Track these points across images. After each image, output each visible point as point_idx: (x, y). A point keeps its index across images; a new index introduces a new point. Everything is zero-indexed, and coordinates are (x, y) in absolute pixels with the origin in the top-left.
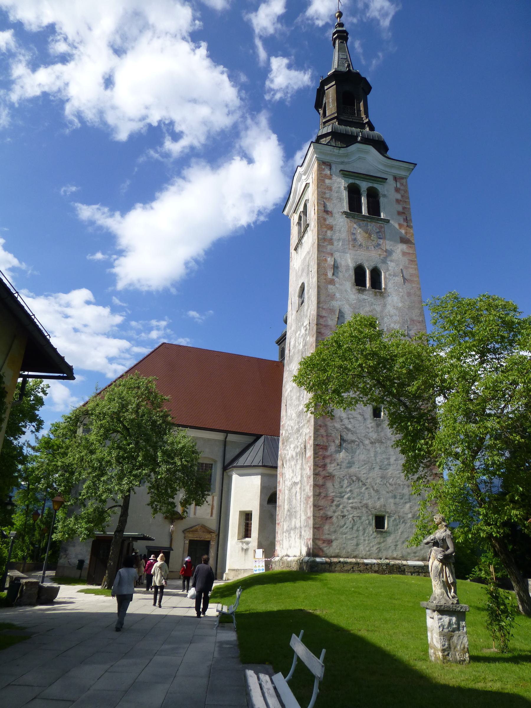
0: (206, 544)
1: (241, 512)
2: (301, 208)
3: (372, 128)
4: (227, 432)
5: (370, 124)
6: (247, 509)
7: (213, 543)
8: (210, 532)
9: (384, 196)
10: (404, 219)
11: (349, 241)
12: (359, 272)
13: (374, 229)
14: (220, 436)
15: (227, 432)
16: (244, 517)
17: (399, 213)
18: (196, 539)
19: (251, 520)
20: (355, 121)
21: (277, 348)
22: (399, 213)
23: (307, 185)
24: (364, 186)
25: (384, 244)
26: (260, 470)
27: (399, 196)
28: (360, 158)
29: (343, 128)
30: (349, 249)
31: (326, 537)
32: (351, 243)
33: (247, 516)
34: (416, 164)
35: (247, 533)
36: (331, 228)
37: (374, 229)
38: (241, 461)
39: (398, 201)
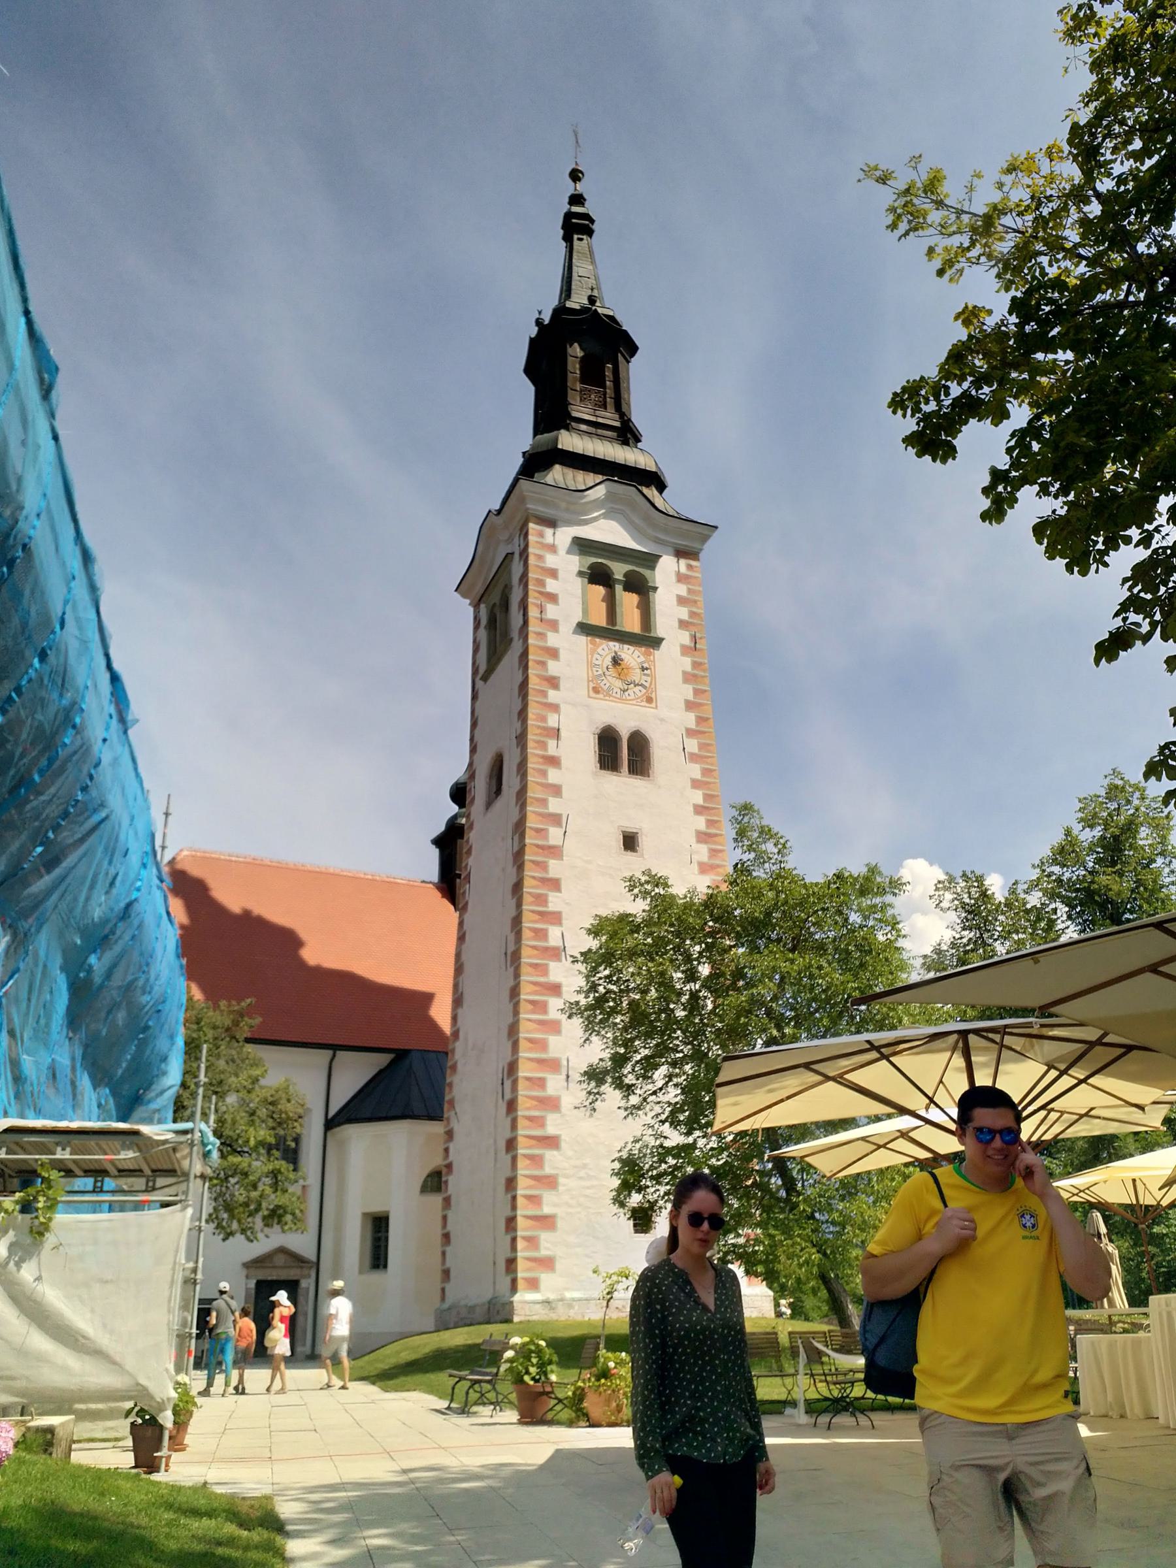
1: (365, 1215)
2: (495, 597)
6: (376, 1208)
8: (298, 1260)
9: (655, 589)
10: (691, 635)
11: (589, 681)
12: (607, 741)
13: (636, 657)
15: (335, 1048)
16: (369, 1227)
17: (683, 624)
18: (269, 1278)
19: (387, 1231)
20: (600, 420)
21: (434, 853)
22: (683, 624)
23: (509, 556)
24: (619, 570)
25: (653, 686)
27: (682, 590)
30: (589, 697)
31: (544, 1252)
32: (592, 685)
33: (379, 1224)
34: (716, 527)
35: (378, 1258)
36: (554, 653)
37: (636, 657)
39: (681, 601)
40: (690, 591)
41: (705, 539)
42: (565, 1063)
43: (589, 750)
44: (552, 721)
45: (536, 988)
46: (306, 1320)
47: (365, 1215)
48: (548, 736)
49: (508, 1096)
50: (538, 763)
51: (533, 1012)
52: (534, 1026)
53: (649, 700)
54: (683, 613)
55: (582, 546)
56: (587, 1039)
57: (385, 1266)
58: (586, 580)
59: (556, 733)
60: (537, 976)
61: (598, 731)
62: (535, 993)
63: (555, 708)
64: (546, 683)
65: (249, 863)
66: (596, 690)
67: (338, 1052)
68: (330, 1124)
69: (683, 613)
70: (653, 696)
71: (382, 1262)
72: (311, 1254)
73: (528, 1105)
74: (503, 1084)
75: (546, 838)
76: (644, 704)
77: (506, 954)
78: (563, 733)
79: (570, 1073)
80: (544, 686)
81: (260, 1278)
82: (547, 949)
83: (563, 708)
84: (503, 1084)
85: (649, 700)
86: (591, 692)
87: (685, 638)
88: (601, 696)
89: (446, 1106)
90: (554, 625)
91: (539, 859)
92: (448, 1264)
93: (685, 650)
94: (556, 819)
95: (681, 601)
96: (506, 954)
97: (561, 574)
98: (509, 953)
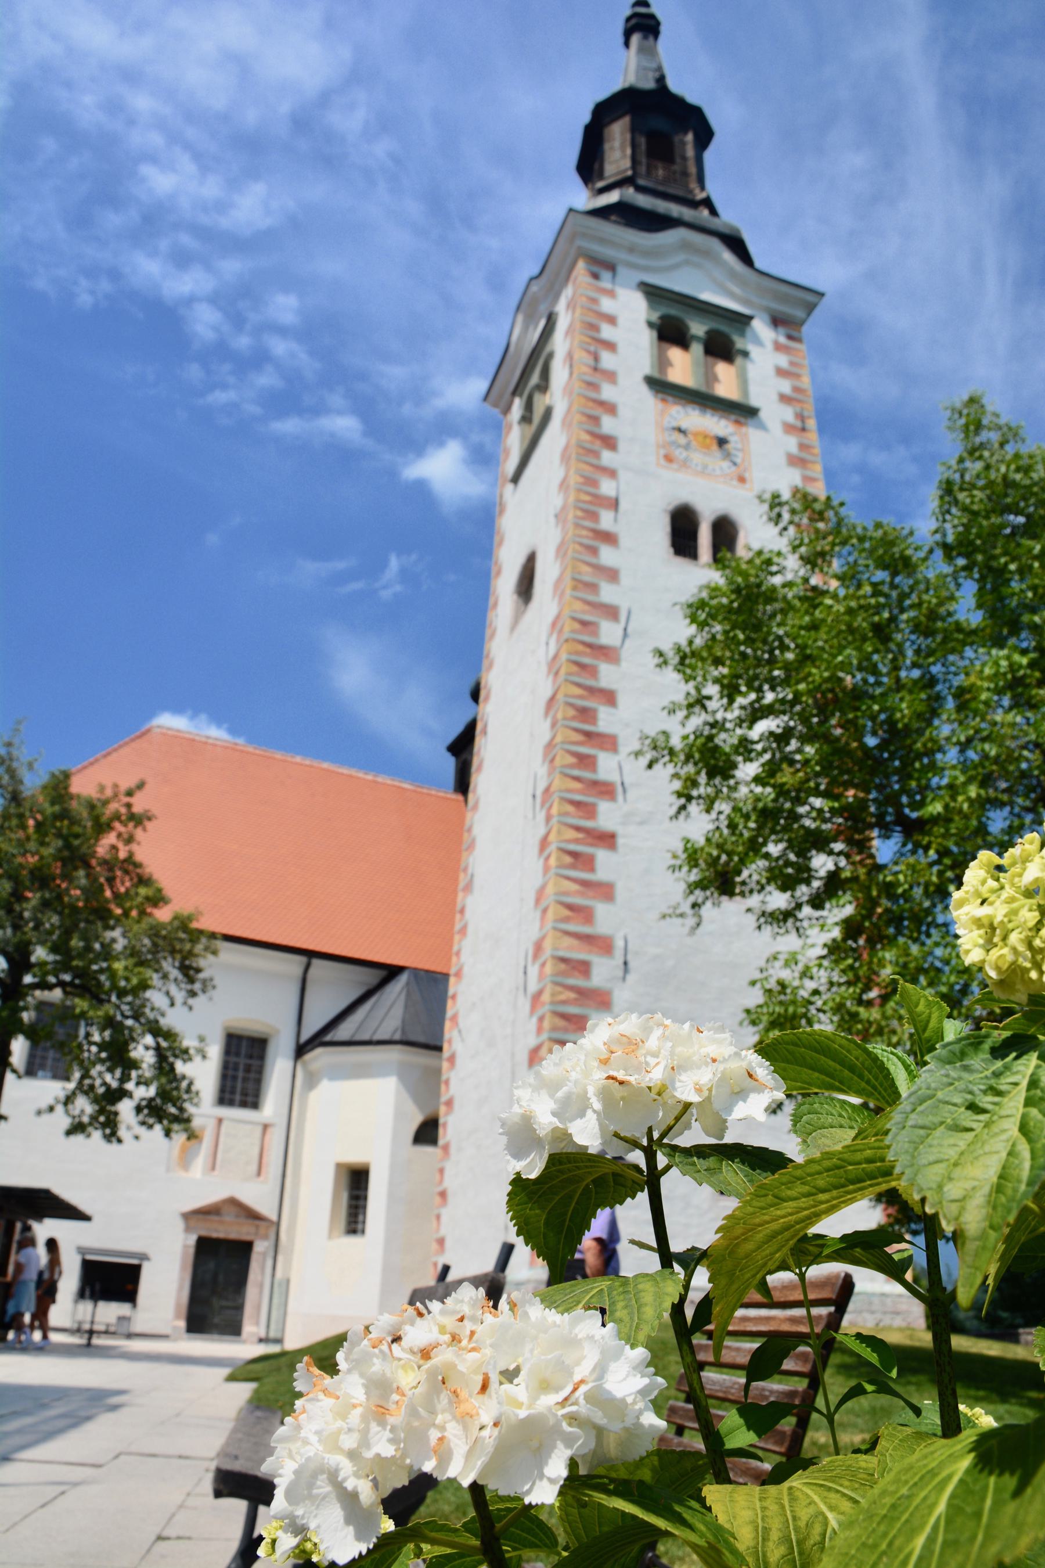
0: (244, 1249)
1: (339, 1166)
3: (714, 212)
4: (311, 955)
5: (708, 203)
6: (355, 1157)
7: (260, 1247)
8: (253, 1216)
14: (294, 965)
16: (345, 1181)
17: (784, 398)
19: (366, 1188)
22: (784, 398)
26: (394, 1055)
28: (687, 262)
29: (643, 201)
32: (662, 452)
38: (344, 1031)
39: (781, 372)
40: (792, 363)
41: (811, 308)
42: (619, 943)
43: (661, 533)
44: (607, 487)
45: (580, 836)
46: (261, 1292)
47: (339, 1166)
48: (601, 505)
49: (533, 986)
50: (587, 537)
51: (573, 867)
52: (575, 887)
53: (742, 480)
54: (785, 386)
55: (653, 293)
56: (683, 808)
57: (363, 1232)
58: (655, 334)
59: (614, 504)
60: (581, 817)
61: (671, 507)
62: (576, 841)
63: (612, 473)
64: (598, 443)
65: (227, 748)
66: (669, 459)
67: (316, 962)
68: (301, 1050)
69: (785, 386)
70: (747, 475)
71: (360, 1226)
72: (266, 1208)
73: (563, 997)
74: (525, 973)
75: (595, 633)
76: (735, 482)
77: (534, 796)
78: (623, 505)
79: (630, 958)
80: (597, 445)
81: (204, 1233)
82: (595, 783)
83: (622, 474)
84: (525, 973)
85: (742, 480)
86: (662, 461)
87: (788, 414)
88: (675, 466)
89: (448, 1025)
90: (611, 376)
91: (586, 660)
92: (443, 1232)
93: (789, 428)
94: (611, 612)
95: (781, 372)
96: (534, 796)
97: (621, 321)
98: (539, 793)
